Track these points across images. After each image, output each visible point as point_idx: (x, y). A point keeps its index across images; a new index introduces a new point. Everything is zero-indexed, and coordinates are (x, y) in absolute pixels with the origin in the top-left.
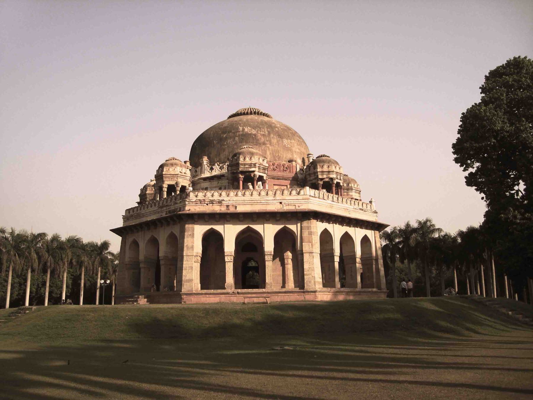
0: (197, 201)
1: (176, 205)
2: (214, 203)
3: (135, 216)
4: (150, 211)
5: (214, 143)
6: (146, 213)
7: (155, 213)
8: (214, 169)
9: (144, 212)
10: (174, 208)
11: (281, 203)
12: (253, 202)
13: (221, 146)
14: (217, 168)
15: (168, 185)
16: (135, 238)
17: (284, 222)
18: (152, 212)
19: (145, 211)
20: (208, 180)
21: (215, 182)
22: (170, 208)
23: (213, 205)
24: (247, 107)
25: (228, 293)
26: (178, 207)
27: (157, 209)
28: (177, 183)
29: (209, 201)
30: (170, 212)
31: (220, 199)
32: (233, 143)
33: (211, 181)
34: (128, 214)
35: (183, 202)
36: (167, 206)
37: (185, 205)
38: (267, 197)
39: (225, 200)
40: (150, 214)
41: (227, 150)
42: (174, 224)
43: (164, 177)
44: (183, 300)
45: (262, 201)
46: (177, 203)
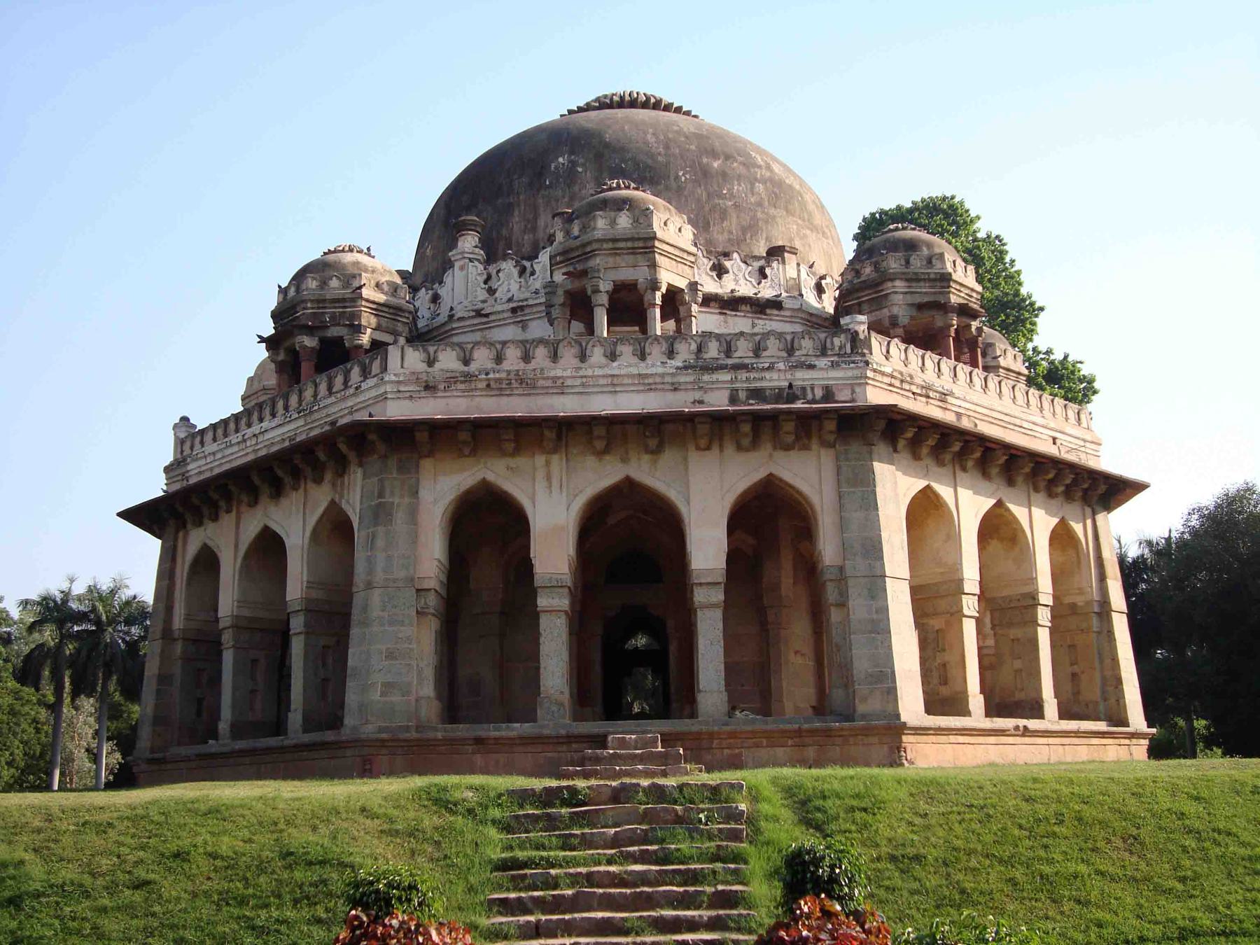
0: (895, 374)
2: (932, 394)
3: (488, 380)
4: (616, 372)
5: (677, 177)
6: (584, 380)
7: (647, 384)
8: (731, 271)
11: (1054, 439)
12: (1007, 419)
13: (709, 195)
14: (739, 270)
15: (669, 284)
16: (491, 477)
17: (1060, 503)
18: (626, 381)
20: (712, 304)
21: (737, 318)
23: (927, 402)
24: (608, 92)
26: (816, 383)
28: (693, 286)
29: (923, 383)
30: (757, 394)
31: (946, 388)
32: (752, 200)
33: (728, 312)
35: (852, 365)
37: (862, 381)
38: (1026, 410)
39: (957, 395)
41: (734, 220)
42: (800, 449)
43: (657, 248)
44: (903, 754)
45: (1025, 425)
46: (812, 367)
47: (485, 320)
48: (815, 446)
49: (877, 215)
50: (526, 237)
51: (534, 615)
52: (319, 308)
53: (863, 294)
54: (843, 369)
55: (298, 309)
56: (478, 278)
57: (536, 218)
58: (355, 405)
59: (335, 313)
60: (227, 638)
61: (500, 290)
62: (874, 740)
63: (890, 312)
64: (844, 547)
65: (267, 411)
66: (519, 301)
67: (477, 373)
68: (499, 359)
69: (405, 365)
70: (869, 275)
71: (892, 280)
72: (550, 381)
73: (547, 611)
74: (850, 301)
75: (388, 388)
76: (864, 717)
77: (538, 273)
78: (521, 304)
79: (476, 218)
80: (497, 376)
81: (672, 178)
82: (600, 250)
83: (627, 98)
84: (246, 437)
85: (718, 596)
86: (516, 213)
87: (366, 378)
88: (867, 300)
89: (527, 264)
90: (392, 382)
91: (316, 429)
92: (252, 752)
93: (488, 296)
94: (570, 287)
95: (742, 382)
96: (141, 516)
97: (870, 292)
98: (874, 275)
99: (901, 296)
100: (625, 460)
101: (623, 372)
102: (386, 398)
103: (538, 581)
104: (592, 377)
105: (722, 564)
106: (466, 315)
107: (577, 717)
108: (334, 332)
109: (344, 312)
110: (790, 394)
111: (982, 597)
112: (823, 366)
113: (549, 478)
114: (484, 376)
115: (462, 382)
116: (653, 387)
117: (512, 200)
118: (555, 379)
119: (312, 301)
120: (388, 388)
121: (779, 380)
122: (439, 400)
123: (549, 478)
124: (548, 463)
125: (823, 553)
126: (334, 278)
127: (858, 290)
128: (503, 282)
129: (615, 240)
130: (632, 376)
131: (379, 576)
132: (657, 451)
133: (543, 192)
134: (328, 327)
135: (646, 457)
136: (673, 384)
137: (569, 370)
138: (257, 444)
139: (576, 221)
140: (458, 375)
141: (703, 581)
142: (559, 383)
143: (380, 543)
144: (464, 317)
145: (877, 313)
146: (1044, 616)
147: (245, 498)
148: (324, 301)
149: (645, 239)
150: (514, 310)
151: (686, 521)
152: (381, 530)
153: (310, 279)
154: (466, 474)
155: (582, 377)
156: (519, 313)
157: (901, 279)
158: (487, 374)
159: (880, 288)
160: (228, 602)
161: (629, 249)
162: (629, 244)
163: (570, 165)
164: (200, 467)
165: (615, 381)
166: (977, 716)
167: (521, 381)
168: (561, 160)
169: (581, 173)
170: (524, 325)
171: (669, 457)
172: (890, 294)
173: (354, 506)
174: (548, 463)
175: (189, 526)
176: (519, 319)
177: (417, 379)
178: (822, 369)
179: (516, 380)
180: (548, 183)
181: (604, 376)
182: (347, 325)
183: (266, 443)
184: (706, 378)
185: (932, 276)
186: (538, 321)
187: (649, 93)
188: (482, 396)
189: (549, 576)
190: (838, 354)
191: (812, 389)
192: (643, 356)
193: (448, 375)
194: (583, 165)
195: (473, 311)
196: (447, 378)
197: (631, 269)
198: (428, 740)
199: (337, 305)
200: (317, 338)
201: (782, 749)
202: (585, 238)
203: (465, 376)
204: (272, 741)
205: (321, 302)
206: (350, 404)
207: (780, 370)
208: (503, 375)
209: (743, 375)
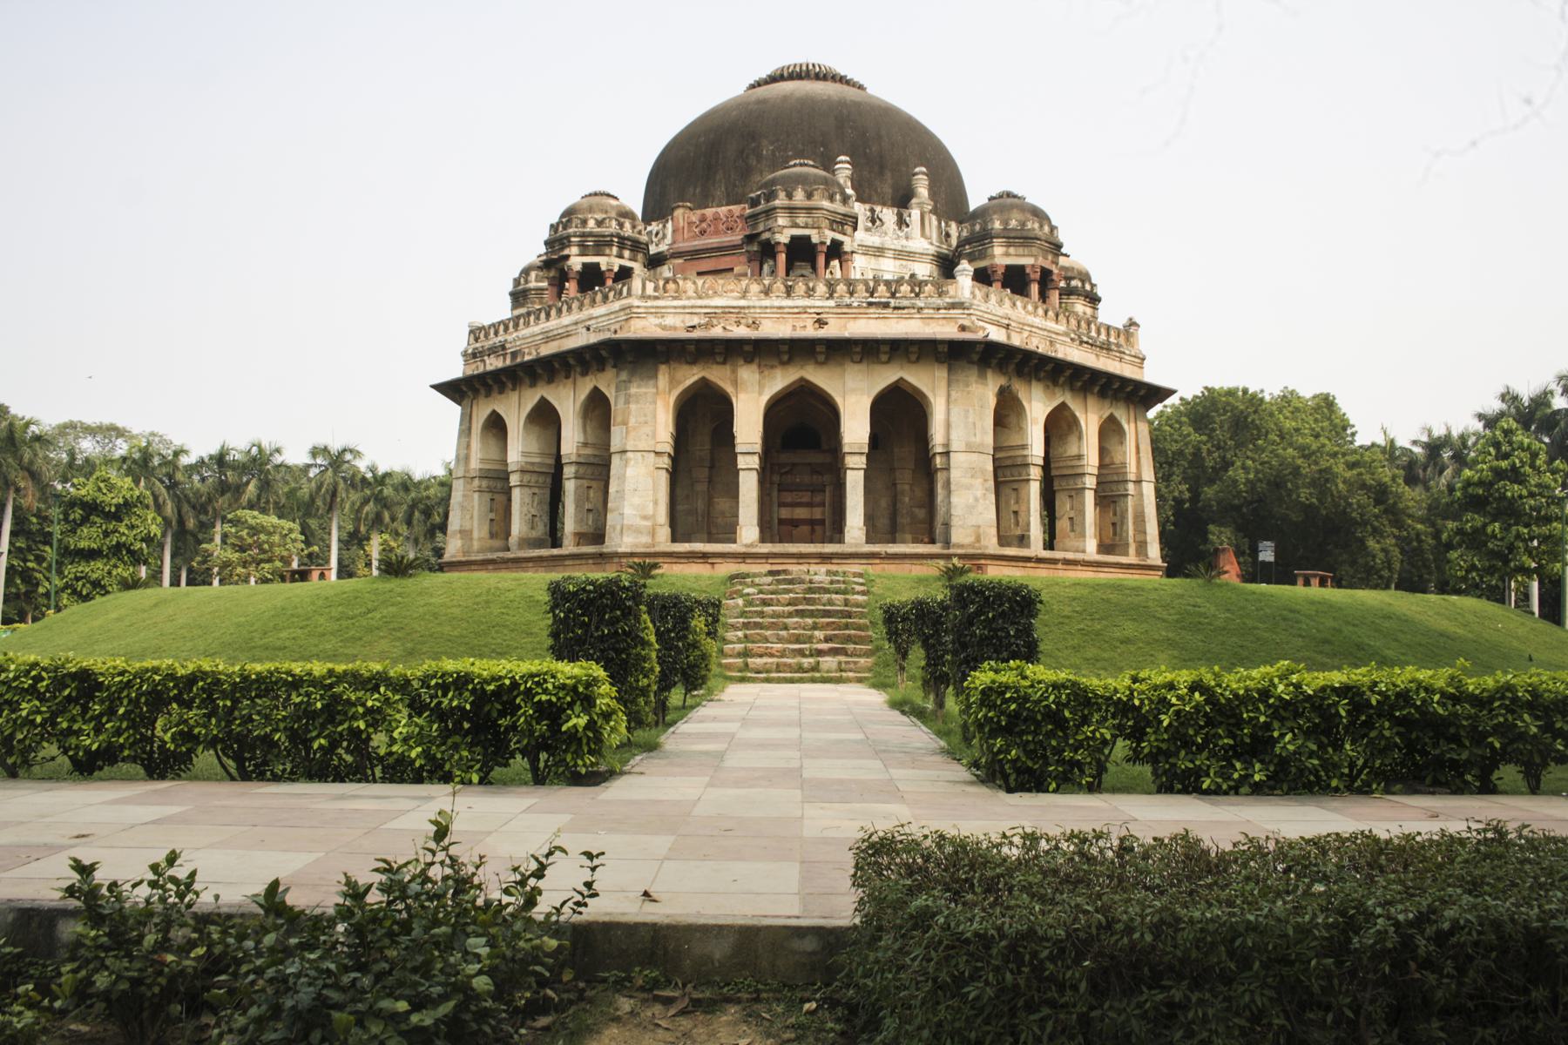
25: (1028, 559)
51: (736, 472)
60: (514, 479)
65: (543, 315)
83: (804, 68)
85: (861, 461)
92: (541, 559)
96: (452, 390)
103: (738, 449)
107: (763, 540)
111: (1046, 467)
146: (1090, 482)
147: (527, 381)
160: (514, 456)
166: (1036, 547)
173: (610, 393)
204: (555, 552)
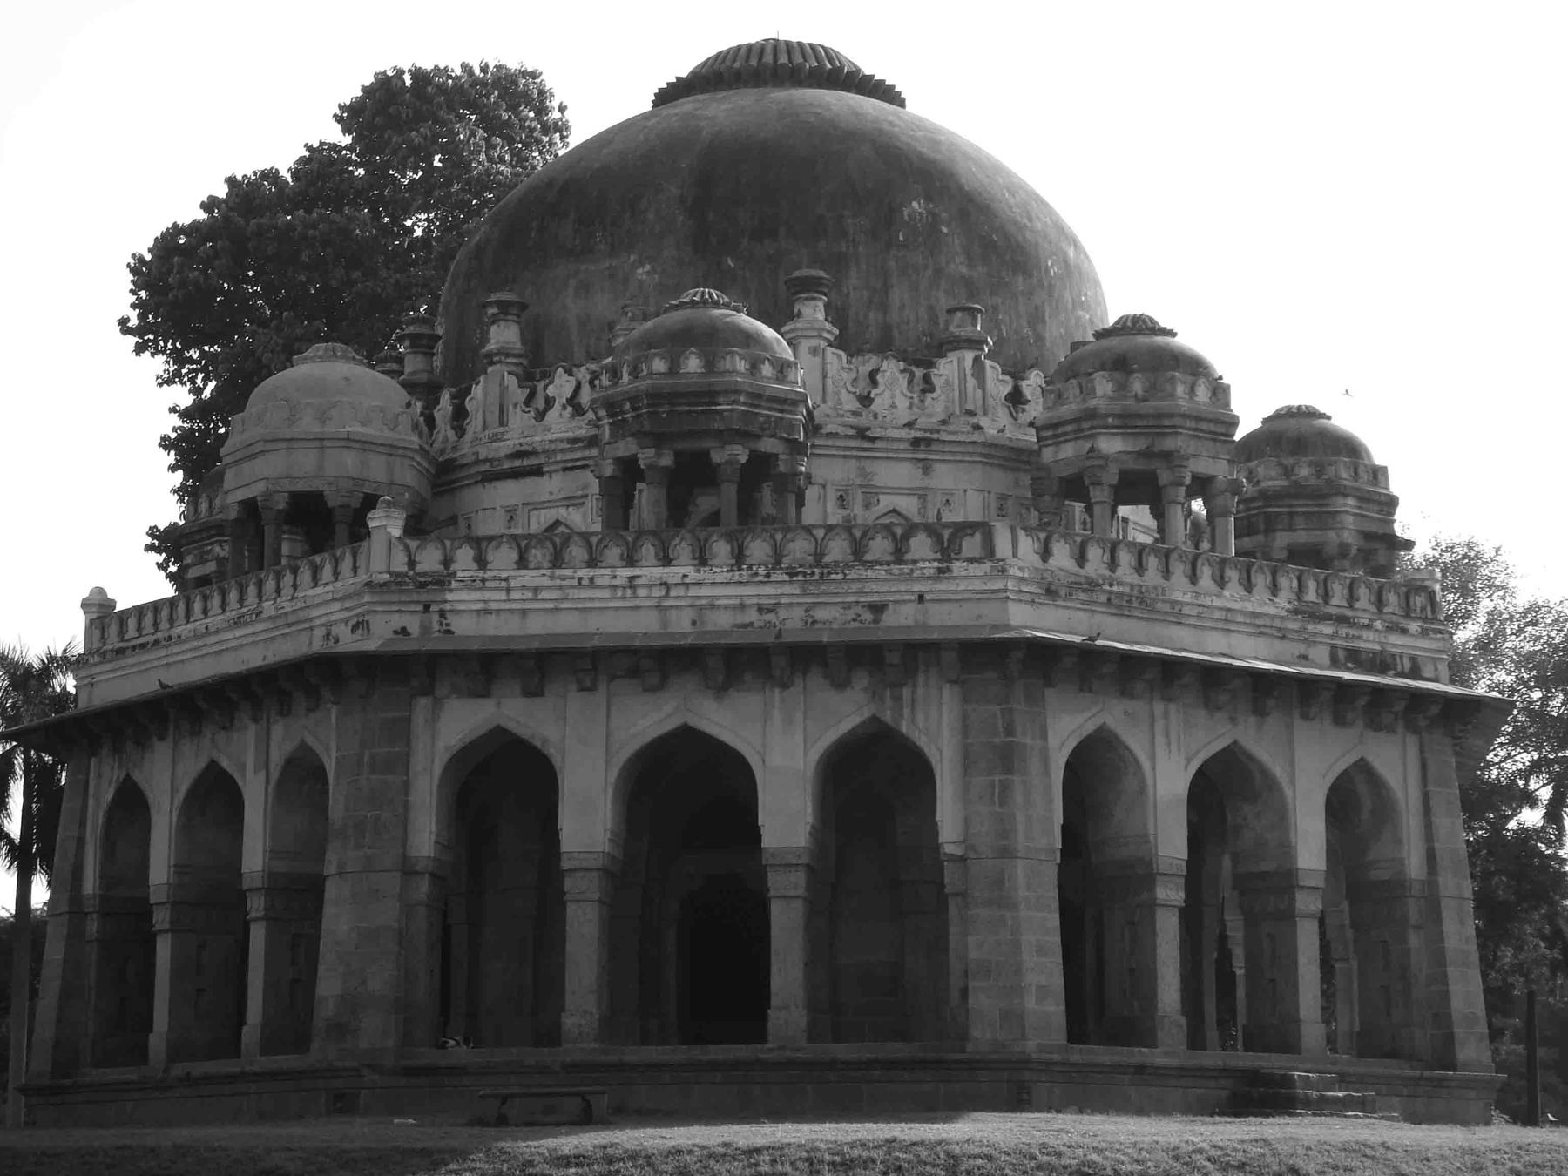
1: (1395, 639)
3: (1111, 592)
6: (1200, 610)
7: (1259, 627)
9: (1188, 598)
10: (1378, 647)
18: (1240, 619)
19: (1198, 594)
22: (1359, 638)
27: (1284, 613)
30: (1355, 658)
34: (1036, 560)
35: (1439, 636)
36: (1342, 620)
40: (1226, 621)
46: (1404, 631)
47: (867, 445)
48: (1400, 729)
49: (408, 82)
50: (872, 315)
52: (751, 405)
53: (1301, 502)
54: (1431, 639)
55: (721, 399)
56: (844, 374)
57: (887, 288)
58: (931, 591)
59: (769, 417)
61: (878, 401)
62: (1473, 1094)
63: (1338, 536)
64: (1431, 857)
66: (925, 431)
67: (1101, 582)
68: (1081, 559)
69: (1020, 553)
70: (1306, 479)
71: (1346, 496)
72: (1168, 605)
73: (1163, 905)
74: (1279, 507)
75: (1011, 585)
76: (1466, 1066)
77: (938, 391)
78: (928, 435)
79: (822, 274)
80: (1121, 589)
81: (1043, 269)
82: (1181, 427)
84: (638, 582)
86: (853, 272)
87: (950, 560)
88: (1304, 513)
89: (919, 372)
90: (1014, 577)
91: (828, 608)
93: (858, 405)
94: (1132, 465)
95: (1341, 638)
97: (1310, 502)
98: (1313, 482)
99: (1350, 519)
100: (1233, 720)
101: (1237, 606)
102: (1008, 598)
104: (1208, 607)
105: (1322, 866)
106: (841, 430)
108: (768, 445)
109: (782, 418)
110: (1381, 663)
112: (1414, 633)
113: (1167, 735)
114: (1107, 588)
115: (1084, 591)
116: (1262, 629)
117: (844, 249)
118: (1174, 603)
119: (748, 394)
120: (1011, 585)
121: (1374, 642)
122: (1060, 611)
123: (1167, 735)
124: (1166, 716)
125: (1407, 862)
126: (767, 362)
127: (1296, 496)
128: (883, 391)
129: (1198, 419)
130: (1242, 612)
131: (1021, 842)
132: (1260, 712)
133: (894, 252)
134: (758, 437)
135: (1252, 719)
136: (1279, 629)
137: (1189, 595)
138: (667, 596)
139: (1136, 375)
140: (1083, 580)
141: (1307, 883)
142: (1177, 608)
143: (1018, 797)
144: (837, 434)
145: (1319, 533)
148: (759, 396)
149: (1216, 421)
150: (916, 442)
151: (1291, 807)
152: (1016, 778)
153: (737, 358)
154: (1087, 715)
155: (1200, 606)
156: (922, 448)
157: (1355, 496)
158: (1111, 585)
159: (1326, 502)
161: (1210, 432)
162: (1212, 427)
163: (930, 218)
164: (485, 602)
165: (1230, 617)
167: (1142, 600)
168: (915, 204)
169: (946, 235)
170: (927, 468)
171: (1274, 722)
172: (1337, 512)
174: (1166, 716)
175: (441, 690)
176: (922, 456)
177: (1042, 579)
178: (1413, 635)
179: (1137, 597)
180: (901, 238)
181: (1221, 609)
182: (781, 438)
183: (704, 602)
184: (1310, 627)
185: (1383, 498)
186: (950, 466)
187: (815, 41)
188: (1079, 609)
189: (1171, 860)
190: (1420, 618)
191: (1401, 657)
192: (1248, 587)
193: (1073, 579)
194: (948, 226)
195: (852, 427)
196: (1072, 583)
197: (1211, 460)
198: (1097, 1065)
199: (775, 406)
200: (747, 452)
201: (1398, 1099)
202: (1151, 406)
203: (1090, 584)
205: (757, 397)
206: (917, 587)
207: (1377, 630)
208: (1127, 590)
209: (1343, 631)
